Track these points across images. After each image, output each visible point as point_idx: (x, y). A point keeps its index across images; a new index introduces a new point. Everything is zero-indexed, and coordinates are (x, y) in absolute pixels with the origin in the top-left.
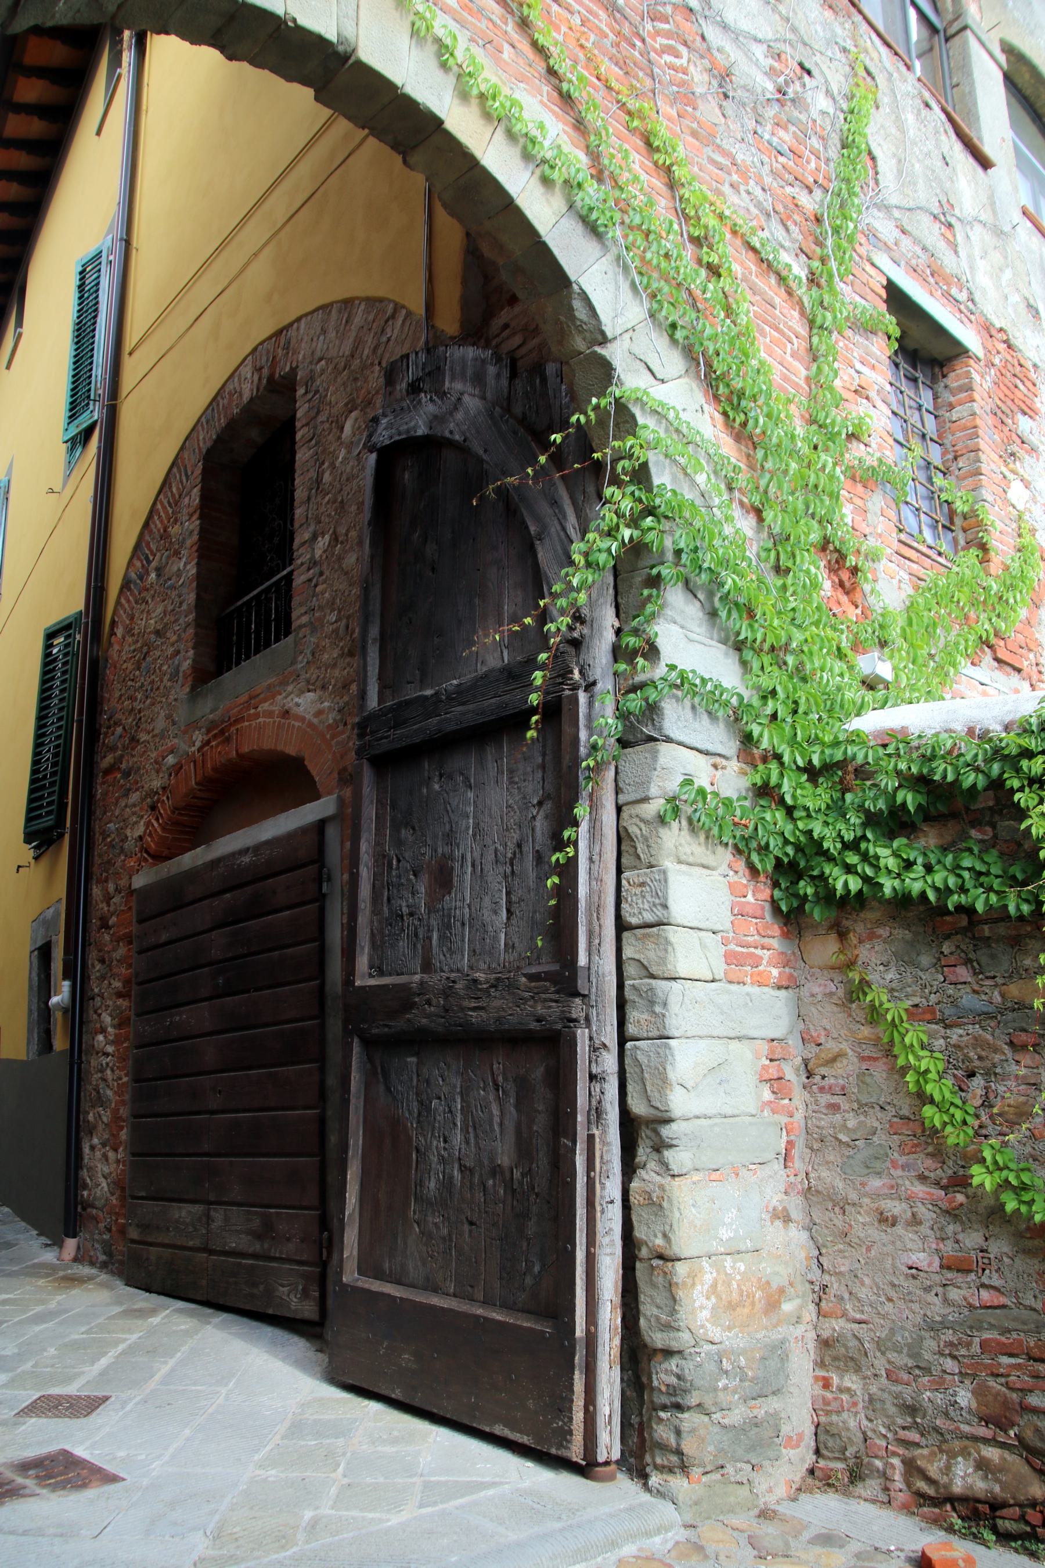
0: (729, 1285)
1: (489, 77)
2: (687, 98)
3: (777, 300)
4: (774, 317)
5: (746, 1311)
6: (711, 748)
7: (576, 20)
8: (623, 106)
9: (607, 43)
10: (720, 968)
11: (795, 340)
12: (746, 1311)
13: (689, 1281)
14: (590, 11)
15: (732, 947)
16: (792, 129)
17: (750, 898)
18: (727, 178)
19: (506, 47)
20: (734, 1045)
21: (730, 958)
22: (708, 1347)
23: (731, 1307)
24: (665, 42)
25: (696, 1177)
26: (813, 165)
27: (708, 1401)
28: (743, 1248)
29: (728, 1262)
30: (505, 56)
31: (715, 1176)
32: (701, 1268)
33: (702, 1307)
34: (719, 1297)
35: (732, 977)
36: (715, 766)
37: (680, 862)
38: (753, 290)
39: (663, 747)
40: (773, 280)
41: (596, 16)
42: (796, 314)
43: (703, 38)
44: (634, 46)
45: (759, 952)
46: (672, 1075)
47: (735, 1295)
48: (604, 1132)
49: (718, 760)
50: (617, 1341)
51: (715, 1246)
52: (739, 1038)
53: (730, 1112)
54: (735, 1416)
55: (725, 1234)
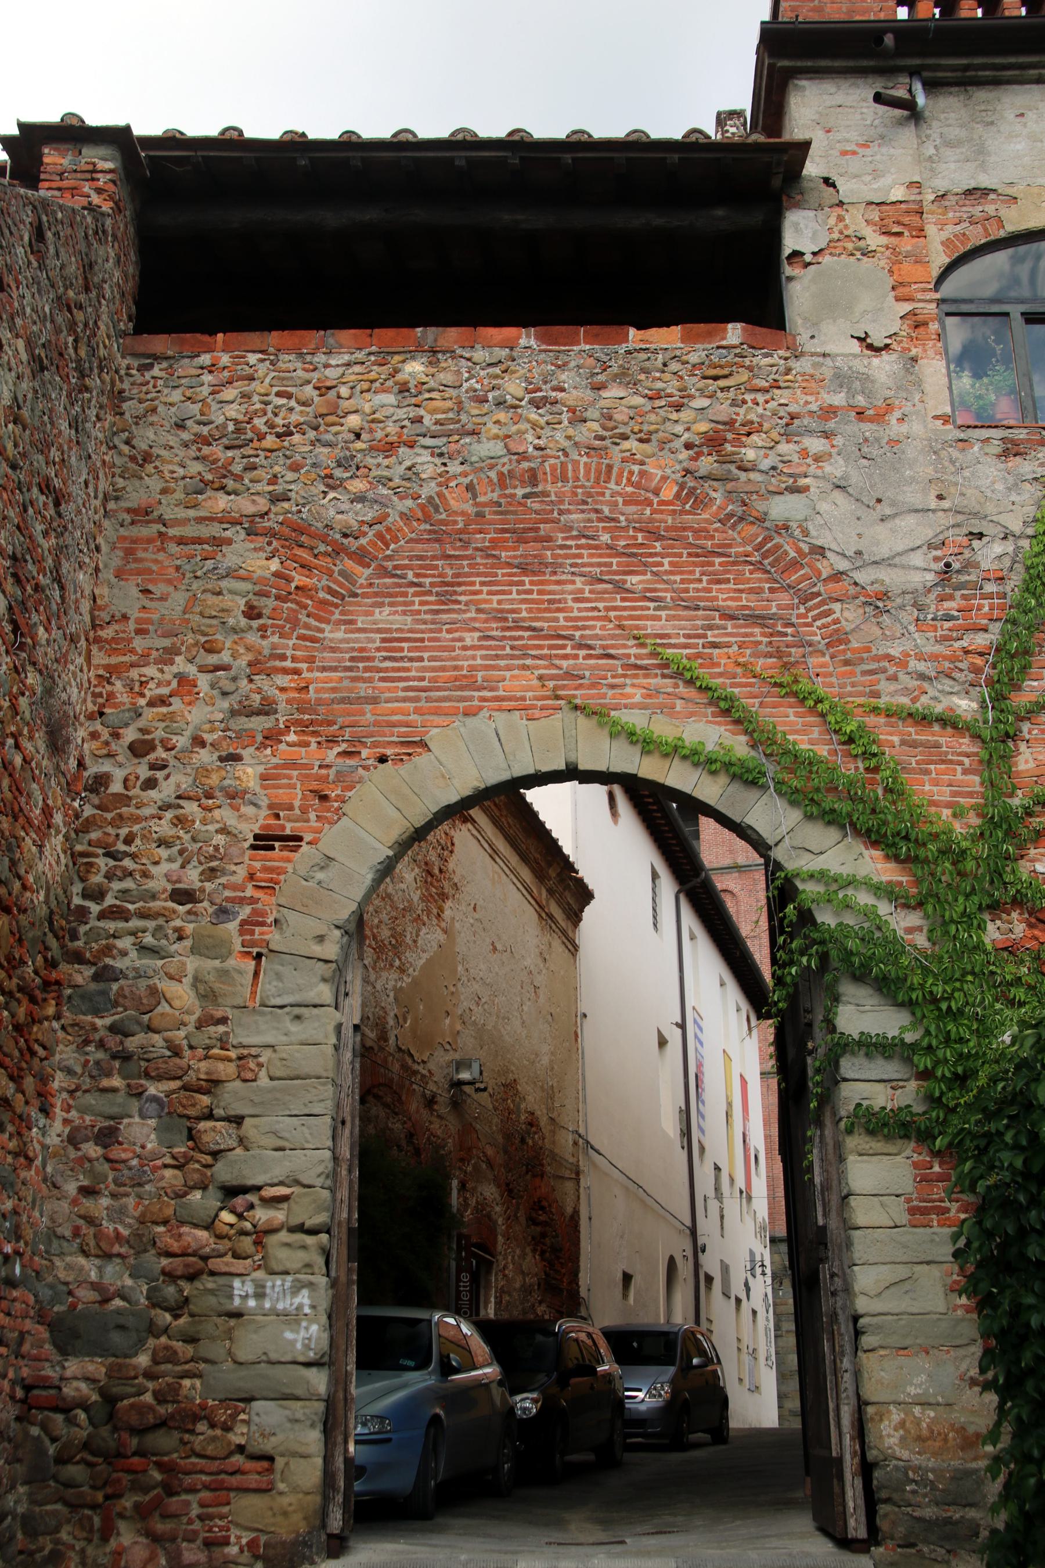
0: (918, 1424)
1: (663, 729)
2: (837, 639)
3: (942, 740)
4: (940, 754)
5: (937, 1444)
6: (885, 1077)
7: (735, 648)
8: (776, 685)
9: (762, 647)
10: (904, 1218)
11: (966, 761)
12: (937, 1444)
13: (877, 1418)
14: (746, 635)
15: (915, 1203)
16: (958, 594)
17: (937, 1168)
18: (882, 676)
19: (679, 702)
20: (918, 1268)
21: (912, 1211)
22: (894, 1462)
23: (920, 1439)
24: (816, 612)
25: (882, 1352)
26: (986, 609)
27: (896, 1496)
28: (932, 1400)
29: (917, 1410)
30: (678, 708)
31: (902, 1352)
32: (889, 1412)
33: (889, 1436)
34: (907, 1431)
35: (915, 1223)
36: (892, 1088)
37: (861, 1155)
38: (914, 744)
39: (844, 1085)
40: (936, 728)
41: (752, 635)
42: (966, 741)
43: (856, 584)
44: (786, 635)
45: (947, 1204)
46: (857, 1288)
47: (925, 1433)
48: (839, 1329)
49: (894, 1084)
50: (857, 1460)
51: (902, 1397)
52: (928, 1263)
53: (916, 1311)
54: (929, 1512)
55: (912, 1390)
